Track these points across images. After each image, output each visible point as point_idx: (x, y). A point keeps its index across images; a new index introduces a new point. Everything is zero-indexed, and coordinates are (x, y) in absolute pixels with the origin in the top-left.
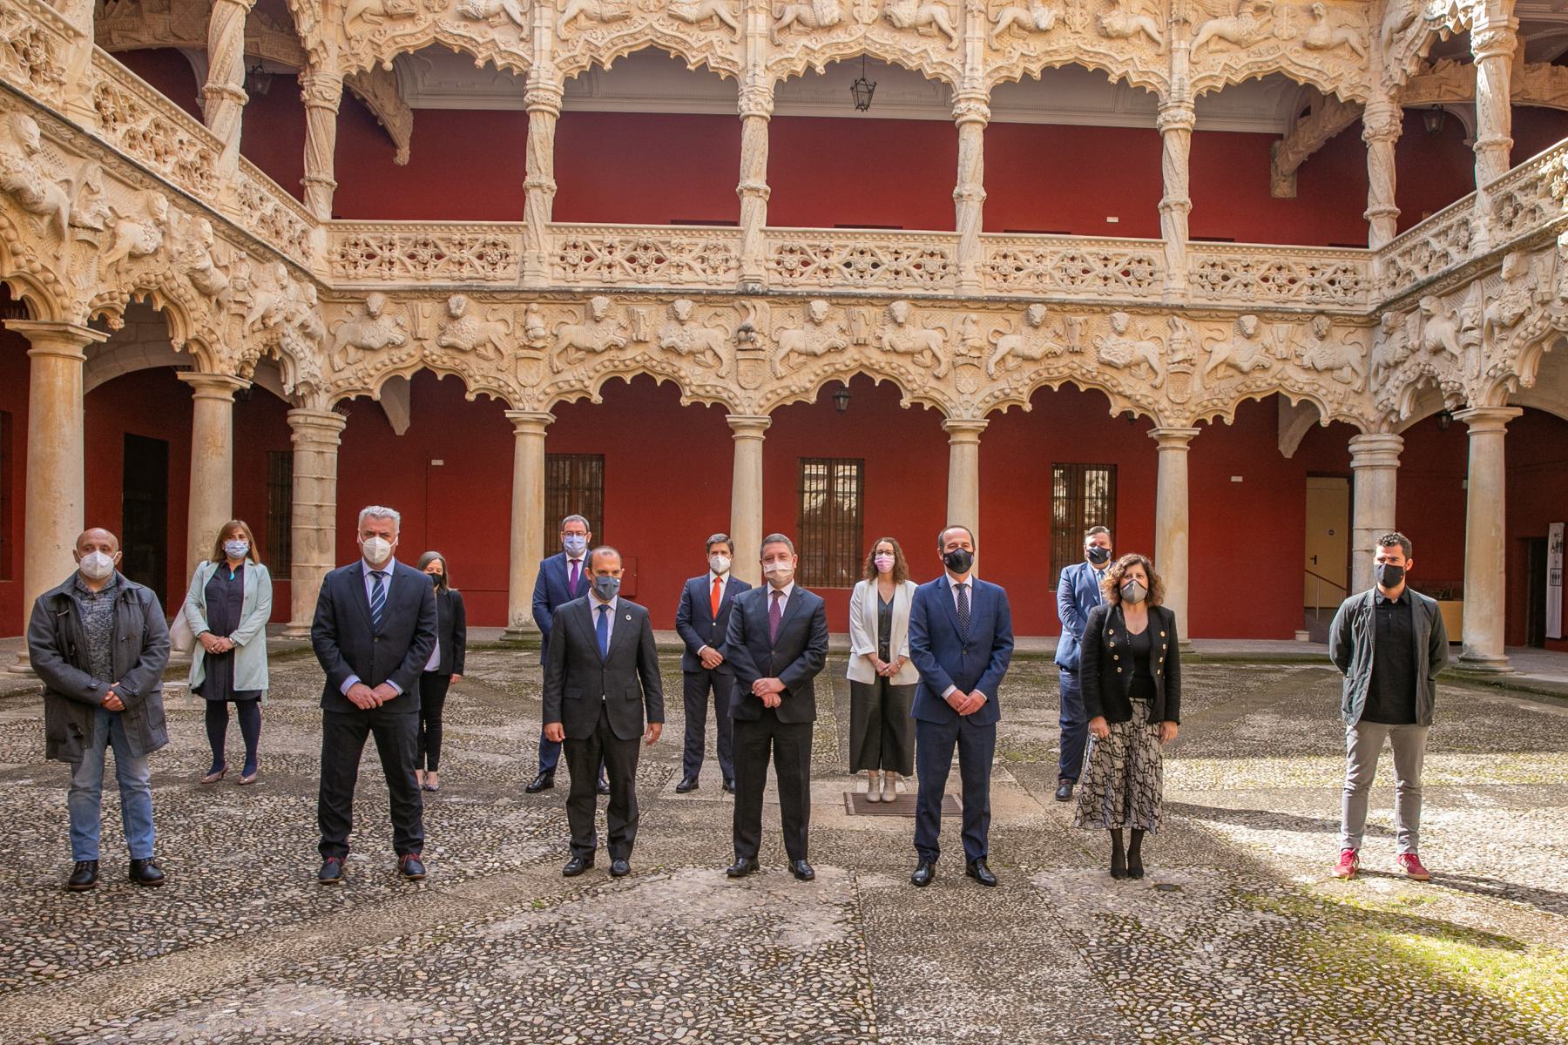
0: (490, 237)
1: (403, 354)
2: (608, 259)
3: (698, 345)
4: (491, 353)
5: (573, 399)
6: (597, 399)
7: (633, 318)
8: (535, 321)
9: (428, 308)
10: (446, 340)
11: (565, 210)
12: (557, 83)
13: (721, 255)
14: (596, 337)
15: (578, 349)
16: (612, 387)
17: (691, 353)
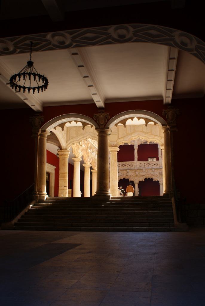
0: (131, 163)
1: (122, 177)
2: (144, 165)
3: (155, 174)
4: (132, 176)
5: (141, 181)
6: (144, 181)
7: (147, 171)
8: (137, 172)
9: (125, 172)
10: (127, 175)
11: (139, 160)
12: (137, 146)
13: (157, 164)
14: (144, 174)
15: (142, 175)
16: (145, 179)
17: (154, 175)
